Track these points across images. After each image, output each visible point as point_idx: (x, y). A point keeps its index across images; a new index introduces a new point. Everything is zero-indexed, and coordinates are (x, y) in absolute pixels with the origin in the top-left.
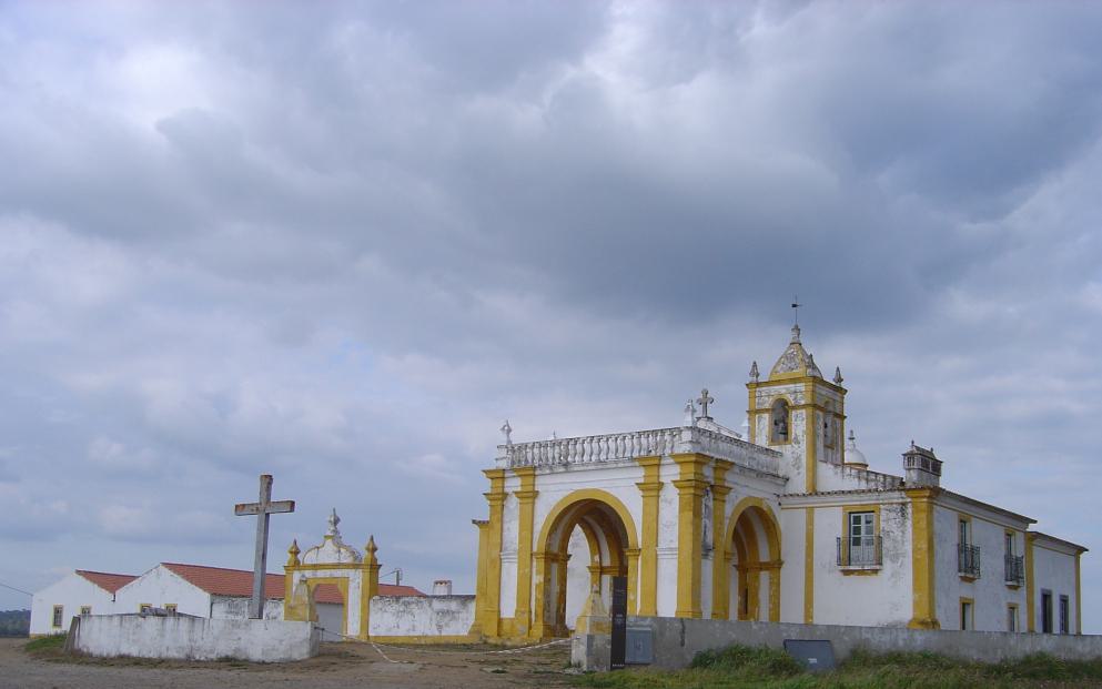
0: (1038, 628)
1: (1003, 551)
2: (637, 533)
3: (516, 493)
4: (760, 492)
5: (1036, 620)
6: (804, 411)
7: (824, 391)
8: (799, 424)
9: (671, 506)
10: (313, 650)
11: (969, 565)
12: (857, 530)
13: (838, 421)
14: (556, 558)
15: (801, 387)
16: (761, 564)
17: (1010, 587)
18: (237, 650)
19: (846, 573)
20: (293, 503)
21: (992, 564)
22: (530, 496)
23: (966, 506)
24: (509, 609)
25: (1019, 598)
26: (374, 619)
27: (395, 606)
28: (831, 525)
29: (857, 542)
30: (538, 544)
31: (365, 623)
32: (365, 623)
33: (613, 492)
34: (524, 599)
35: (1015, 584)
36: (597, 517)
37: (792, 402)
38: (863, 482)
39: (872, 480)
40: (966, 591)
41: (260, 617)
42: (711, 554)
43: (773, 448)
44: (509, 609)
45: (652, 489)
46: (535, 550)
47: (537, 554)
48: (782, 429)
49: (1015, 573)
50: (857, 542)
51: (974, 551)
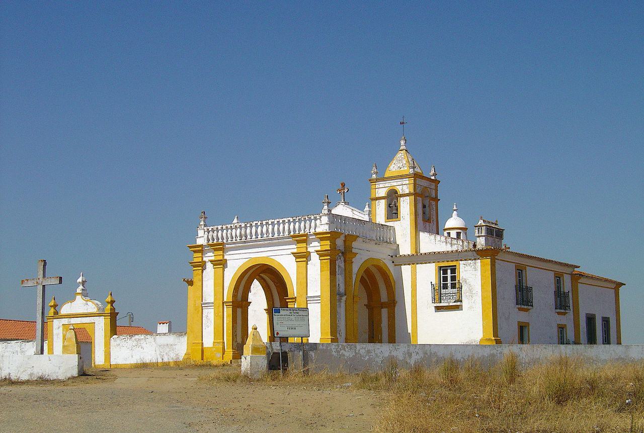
0: (583, 336)
1: (553, 288)
2: (293, 289)
3: (211, 261)
4: (382, 254)
5: (581, 334)
6: (408, 198)
7: (424, 183)
8: (406, 206)
9: (316, 269)
10: (79, 372)
11: (524, 297)
12: (445, 279)
13: (433, 203)
14: (240, 304)
15: (406, 181)
16: (382, 304)
17: (559, 313)
18: (31, 375)
19: (438, 309)
20: (61, 278)
21: (543, 296)
22: (221, 264)
23: (522, 259)
24: (209, 341)
25: (567, 320)
26: (114, 352)
27: (130, 342)
28: (428, 274)
29: (445, 287)
30: (228, 296)
31: (108, 355)
32: (108, 355)
33: (277, 259)
34: (219, 332)
35: (562, 311)
36: (270, 277)
37: (400, 192)
38: (449, 245)
39: (454, 244)
40: (523, 317)
41: (42, 353)
42: (344, 298)
43: (388, 224)
44: (209, 341)
45: (303, 257)
46: (225, 300)
47: (226, 302)
48: (393, 212)
49: (562, 302)
50: (445, 287)
51: (529, 290)
